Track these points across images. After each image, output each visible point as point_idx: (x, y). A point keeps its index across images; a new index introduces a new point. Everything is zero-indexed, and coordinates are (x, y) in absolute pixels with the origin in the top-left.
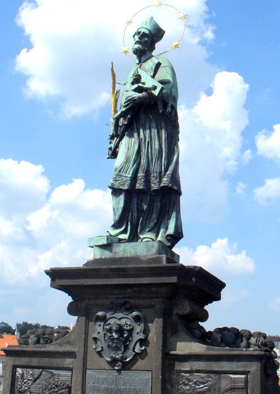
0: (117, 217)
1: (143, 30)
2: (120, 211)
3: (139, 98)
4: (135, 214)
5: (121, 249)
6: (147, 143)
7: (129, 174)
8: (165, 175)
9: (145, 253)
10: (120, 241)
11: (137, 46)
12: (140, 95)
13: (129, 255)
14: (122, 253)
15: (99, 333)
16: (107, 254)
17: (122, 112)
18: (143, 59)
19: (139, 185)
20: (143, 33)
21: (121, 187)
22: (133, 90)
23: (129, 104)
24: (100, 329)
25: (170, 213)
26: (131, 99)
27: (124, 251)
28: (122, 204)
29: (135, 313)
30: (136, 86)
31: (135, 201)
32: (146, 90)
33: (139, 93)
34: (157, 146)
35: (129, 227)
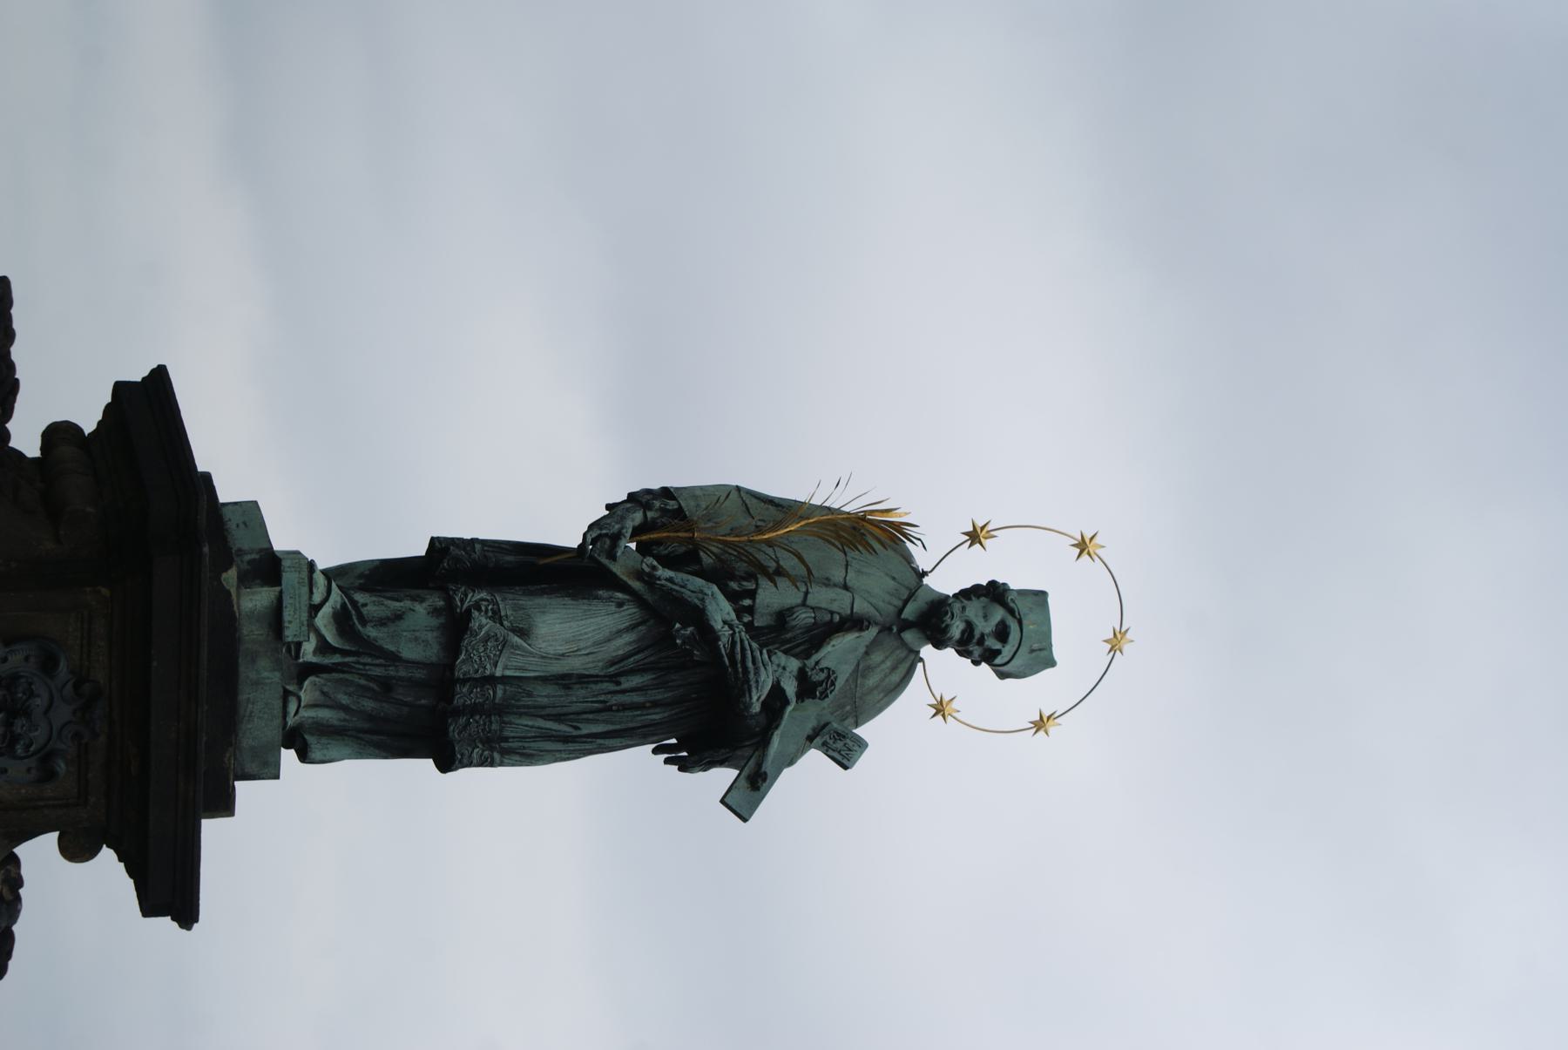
0: (371, 632)
1: (1007, 651)
2: (391, 648)
3: (748, 706)
4: (378, 672)
5: (266, 674)
6: (602, 698)
7: (506, 668)
8: (492, 749)
9: (246, 742)
10: (299, 645)
11: (956, 630)
12: (756, 708)
13: (242, 697)
14: (253, 675)
15: (5, 660)
16: (252, 633)
17: (718, 639)
18: (908, 636)
19: (464, 696)
20: (998, 652)
21: (462, 657)
22: (778, 682)
23: (736, 671)
24: (16, 659)
25: (375, 738)
26: (747, 681)
27: (257, 683)
28: (409, 652)
29: (61, 766)
30: (790, 688)
31: (419, 674)
32: (765, 742)
33: (765, 705)
34: (586, 729)
35: (337, 659)
